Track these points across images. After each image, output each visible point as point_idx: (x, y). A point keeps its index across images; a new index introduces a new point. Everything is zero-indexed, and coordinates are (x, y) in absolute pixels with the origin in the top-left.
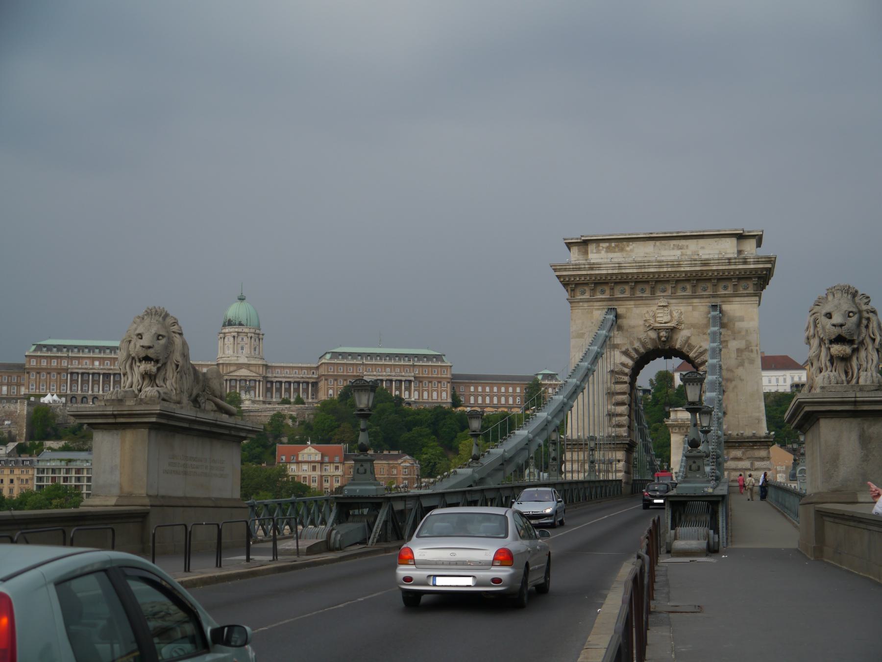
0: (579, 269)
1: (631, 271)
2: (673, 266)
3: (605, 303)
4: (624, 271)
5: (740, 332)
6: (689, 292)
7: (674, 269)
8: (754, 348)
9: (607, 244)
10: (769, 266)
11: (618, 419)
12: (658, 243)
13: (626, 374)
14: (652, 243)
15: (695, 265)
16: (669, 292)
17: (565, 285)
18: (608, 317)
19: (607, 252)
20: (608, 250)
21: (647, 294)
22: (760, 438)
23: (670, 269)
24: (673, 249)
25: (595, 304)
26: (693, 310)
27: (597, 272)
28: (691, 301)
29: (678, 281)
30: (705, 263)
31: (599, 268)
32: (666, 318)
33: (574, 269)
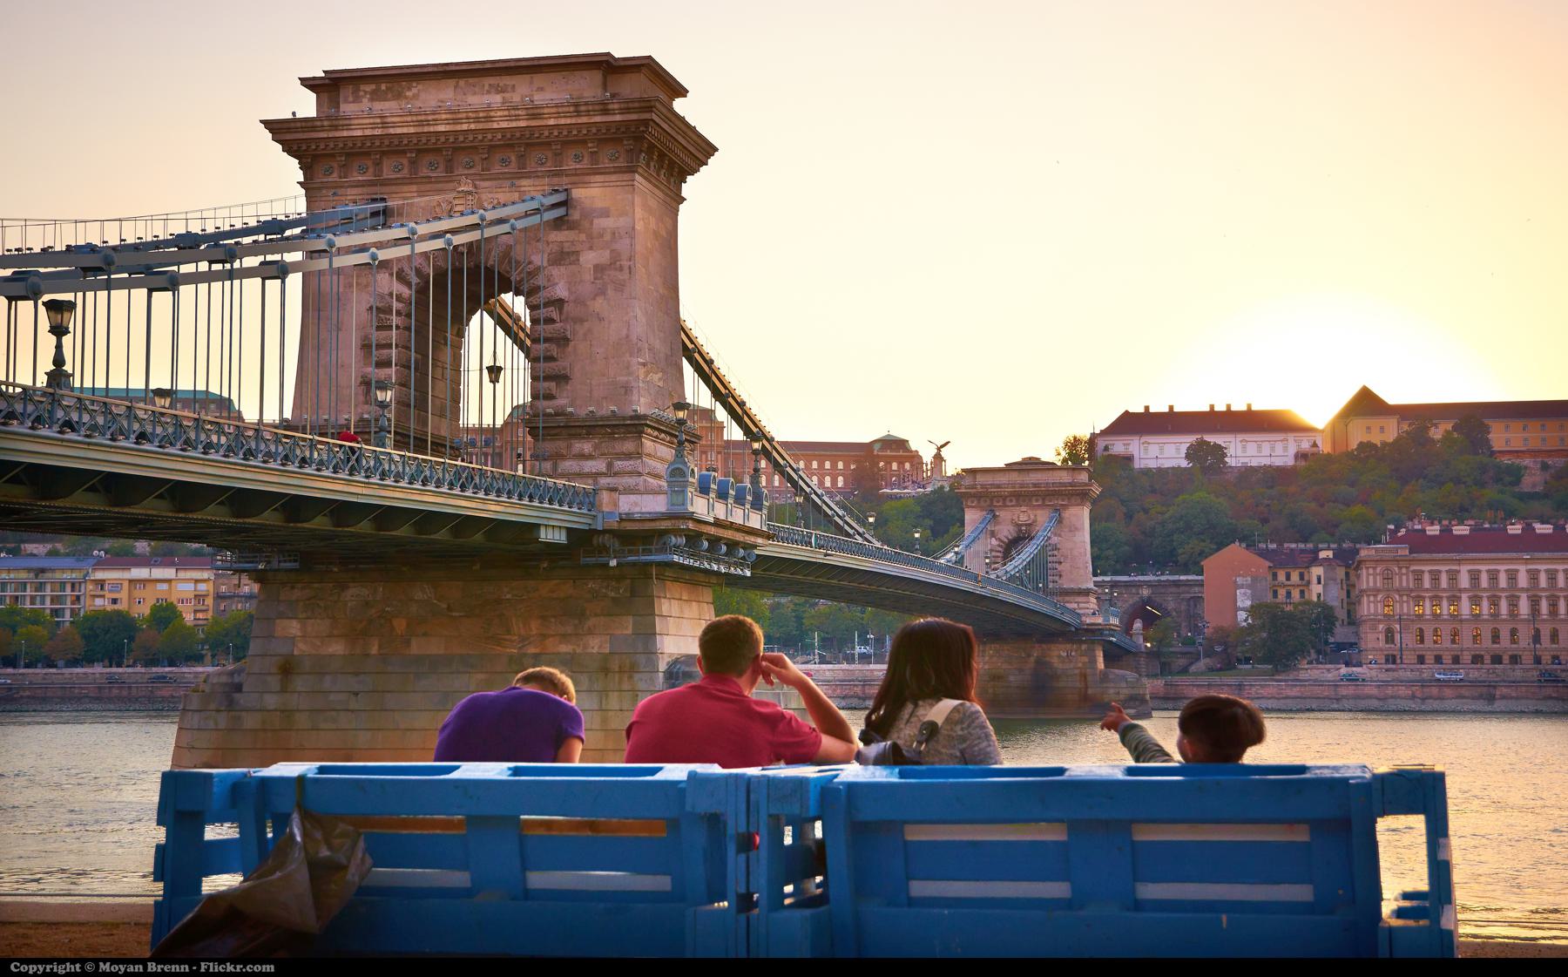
1: (405, 130)
2: (477, 120)
3: (365, 190)
4: (392, 131)
5: (602, 236)
6: (513, 168)
7: (480, 126)
8: (626, 264)
9: (373, 87)
12: (462, 82)
14: (452, 82)
19: (372, 100)
20: (376, 96)
21: (440, 173)
22: (624, 418)
23: (473, 126)
27: (345, 134)
28: (517, 182)
29: (492, 148)
31: (348, 127)
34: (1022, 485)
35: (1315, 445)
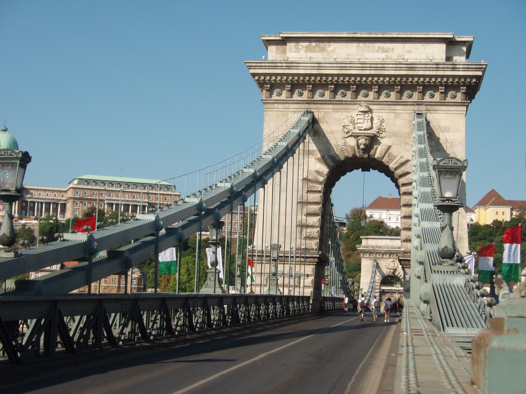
0: (276, 67)
2: (376, 69)
10: (480, 73)
11: (309, 230)
12: (361, 45)
13: (320, 183)
15: (400, 69)
17: (261, 85)
18: (302, 118)
19: (306, 51)
20: (308, 50)
23: (373, 72)
24: (377, 51)
25: (291, 106)
26: (396, 117)
30: (411, 66)
31: (297, 68)
32: (367, 125)
33: (269, 67)
34: (392, 247)
35: (472, 220)
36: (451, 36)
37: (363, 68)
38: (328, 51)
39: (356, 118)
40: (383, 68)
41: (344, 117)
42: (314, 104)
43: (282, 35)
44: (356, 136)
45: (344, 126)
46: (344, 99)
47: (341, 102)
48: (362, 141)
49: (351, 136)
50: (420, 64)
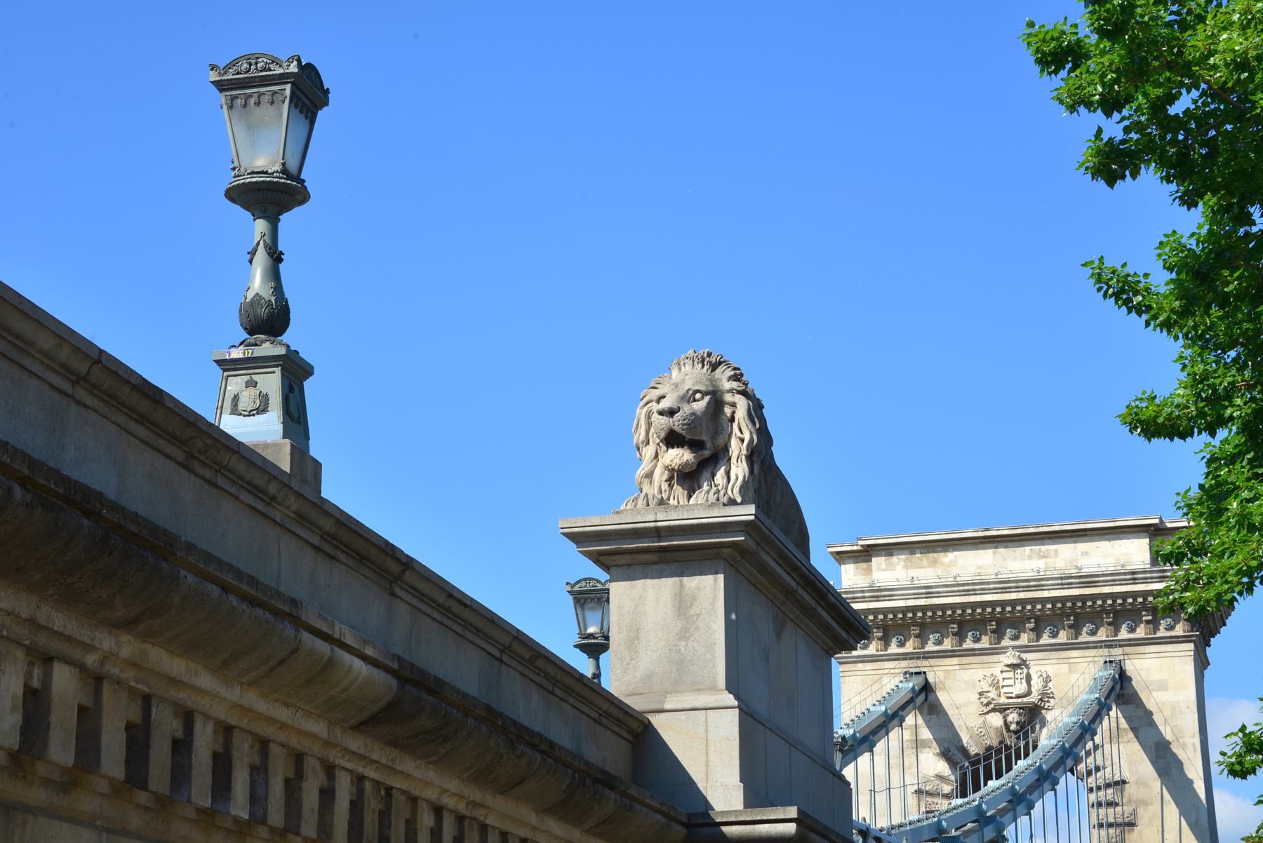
15: (1070, 586)
16: (1024, 639)
19: (906, 567)
23: (1022, 595)
26: (1070, 671)
31: (890, 598)
32: (1020, 688)
36: (1157, 521)
37: (1005, 590)
38: (943, 564)
39: (1000, 677)
40: (1040, 588)
41: (981, 677)
42: (925, 658)
43: (861, 543)
44: (1002, 709)
45: (981, 694)
46: (977, 646)
47: (972, 652)
48: (1013, 717)
49: (993, 710)
50: (1103, 575)
